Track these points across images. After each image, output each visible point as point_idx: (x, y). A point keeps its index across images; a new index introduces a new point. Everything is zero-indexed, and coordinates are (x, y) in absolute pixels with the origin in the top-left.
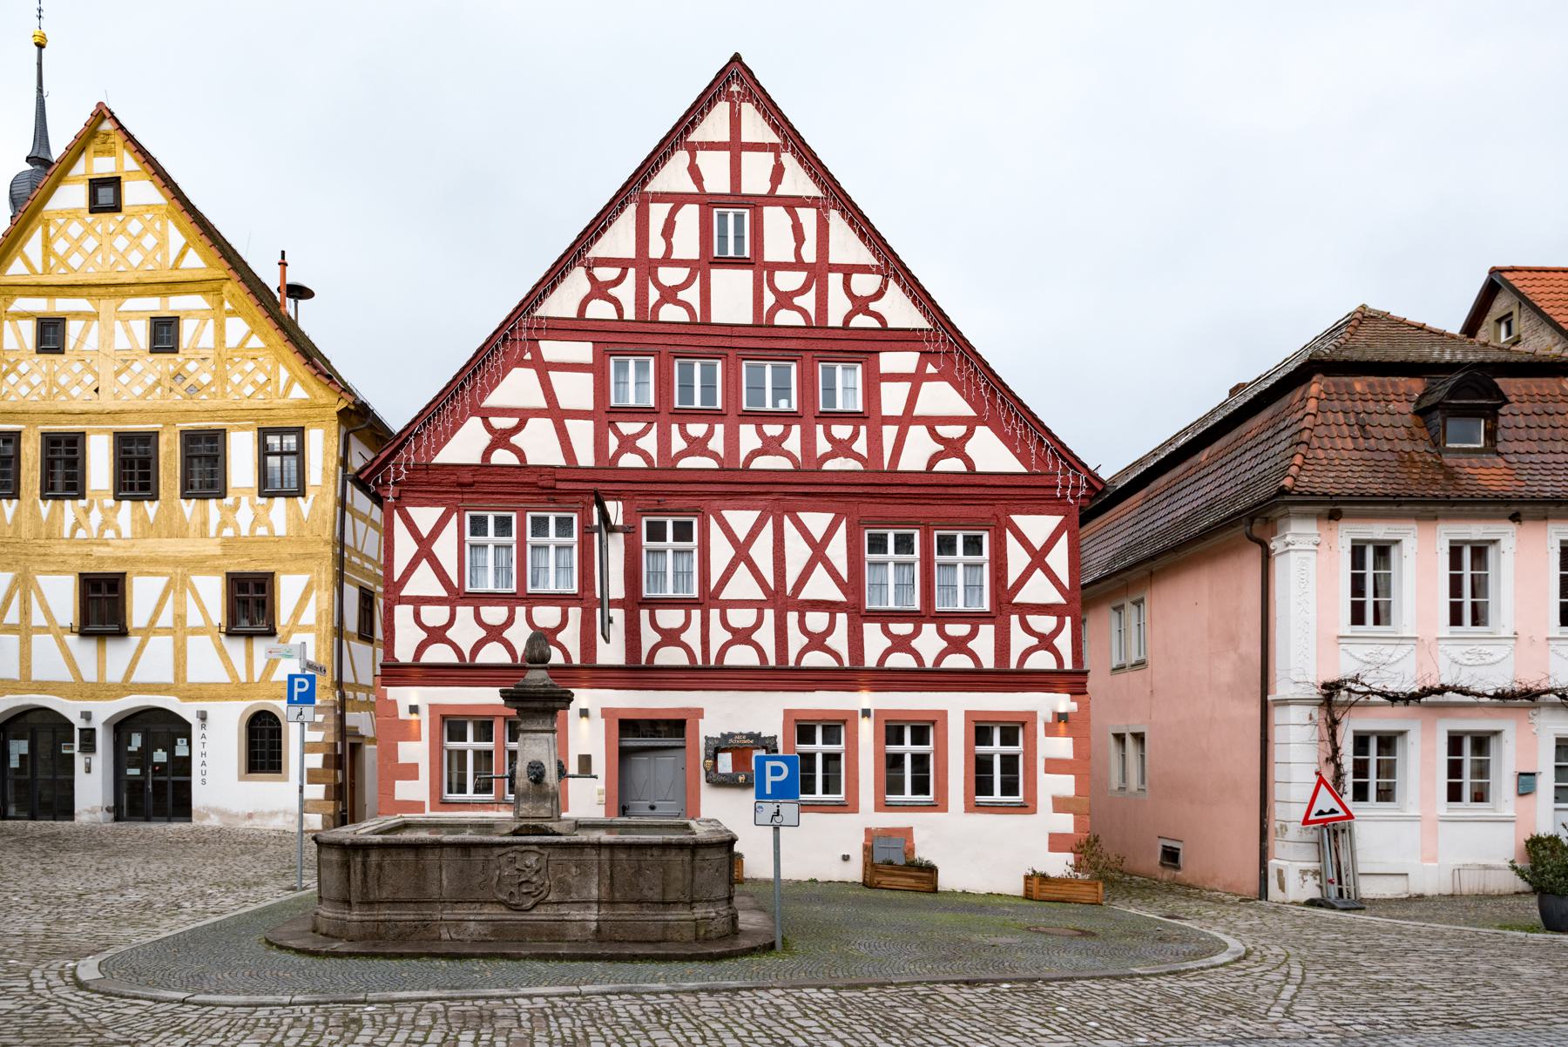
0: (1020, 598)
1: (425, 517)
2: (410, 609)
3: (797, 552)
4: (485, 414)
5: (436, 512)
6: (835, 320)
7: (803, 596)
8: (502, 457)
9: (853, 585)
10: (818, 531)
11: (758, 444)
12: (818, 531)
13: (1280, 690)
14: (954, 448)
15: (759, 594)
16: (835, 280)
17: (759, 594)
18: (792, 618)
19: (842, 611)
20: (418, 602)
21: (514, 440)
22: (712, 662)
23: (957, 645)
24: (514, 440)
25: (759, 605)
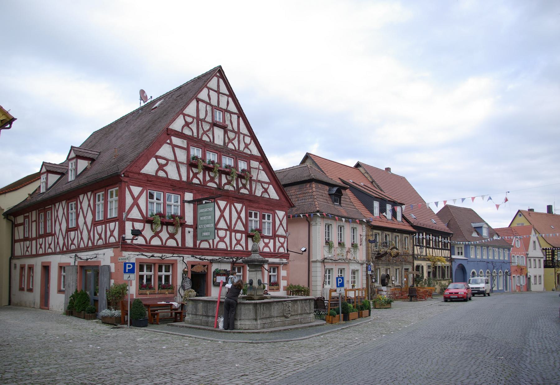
0: (277, 233)
1: (136, 190)
2: (131, 223)
3: (235, 215)
4: (157, 157)
5: (140, 189)
6: (242, 148)
7: (235, 229)
8: (161, 174)
9: (246, 226)
10: (239, 208)
11: (226, 181)
12: (239, 209)
13: (313, 259)
14: (266, 190)
15: (227, 228)
16: (242, 136)
17: (227, 228)
18: (233, 234)
19: (244, 234)
20: (134, 220)
21: (165, 168)
22: (215, 247)
23: (266, 245)
24: (165, 168)
25: (226, 230)
